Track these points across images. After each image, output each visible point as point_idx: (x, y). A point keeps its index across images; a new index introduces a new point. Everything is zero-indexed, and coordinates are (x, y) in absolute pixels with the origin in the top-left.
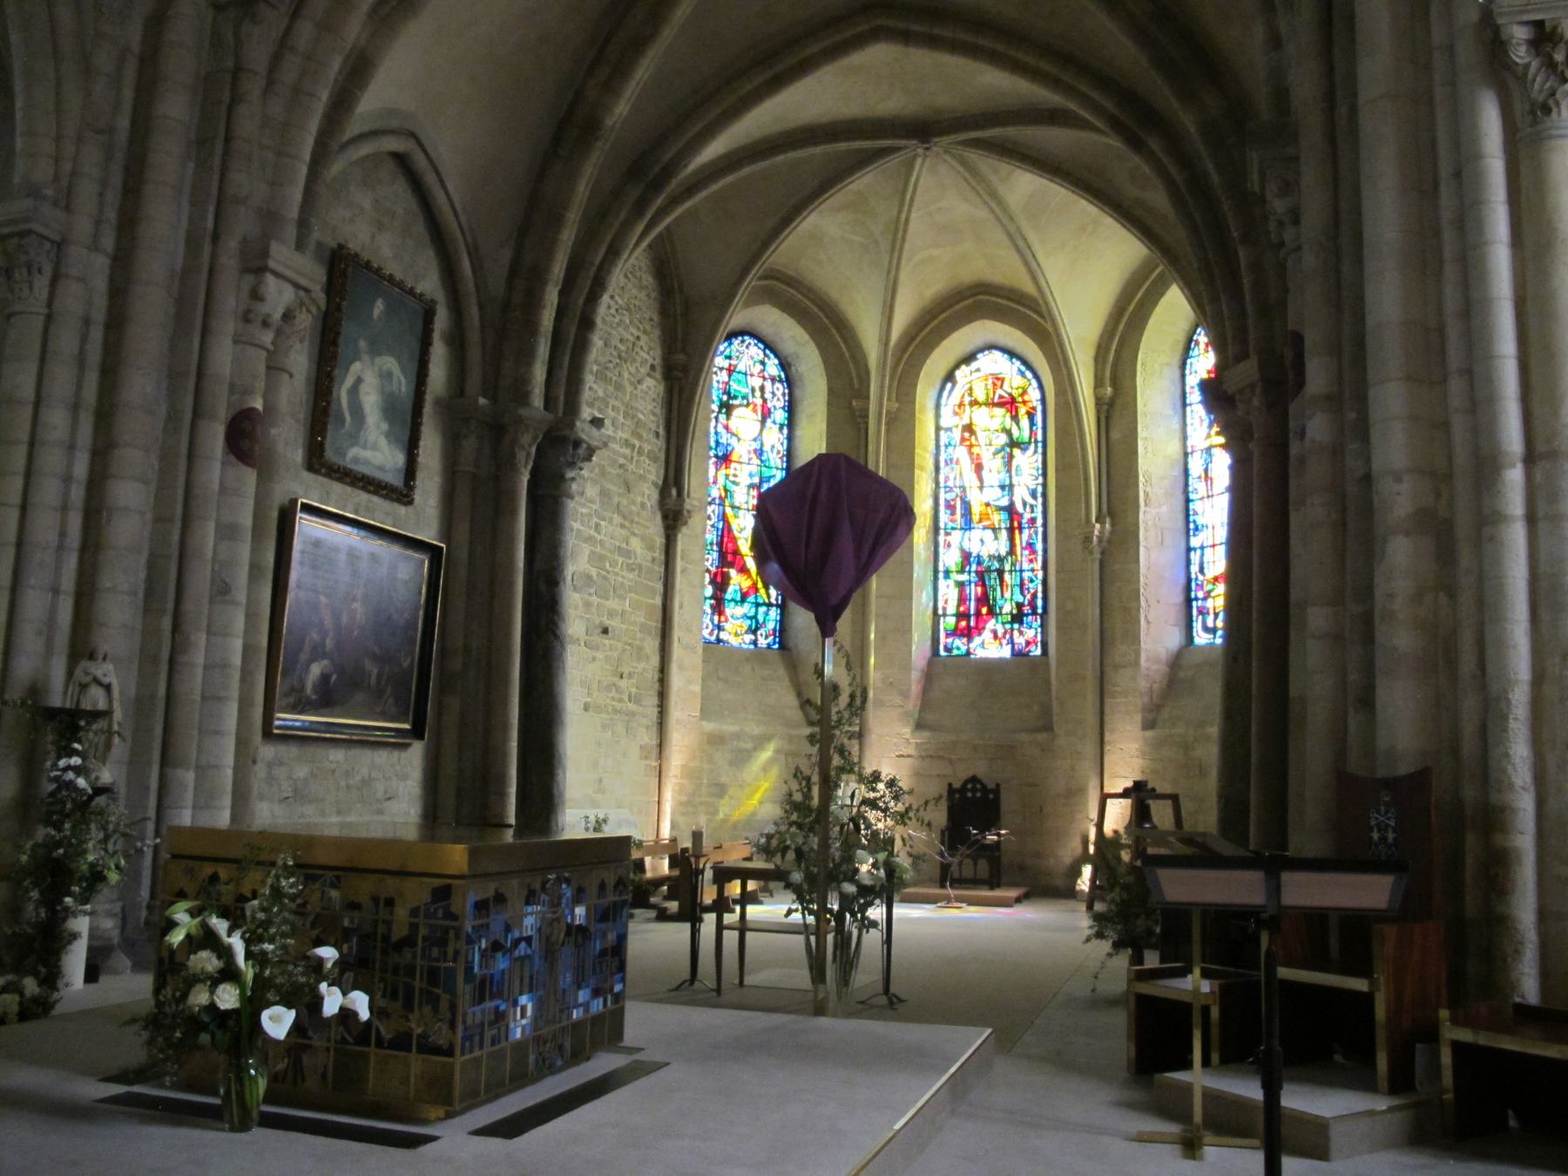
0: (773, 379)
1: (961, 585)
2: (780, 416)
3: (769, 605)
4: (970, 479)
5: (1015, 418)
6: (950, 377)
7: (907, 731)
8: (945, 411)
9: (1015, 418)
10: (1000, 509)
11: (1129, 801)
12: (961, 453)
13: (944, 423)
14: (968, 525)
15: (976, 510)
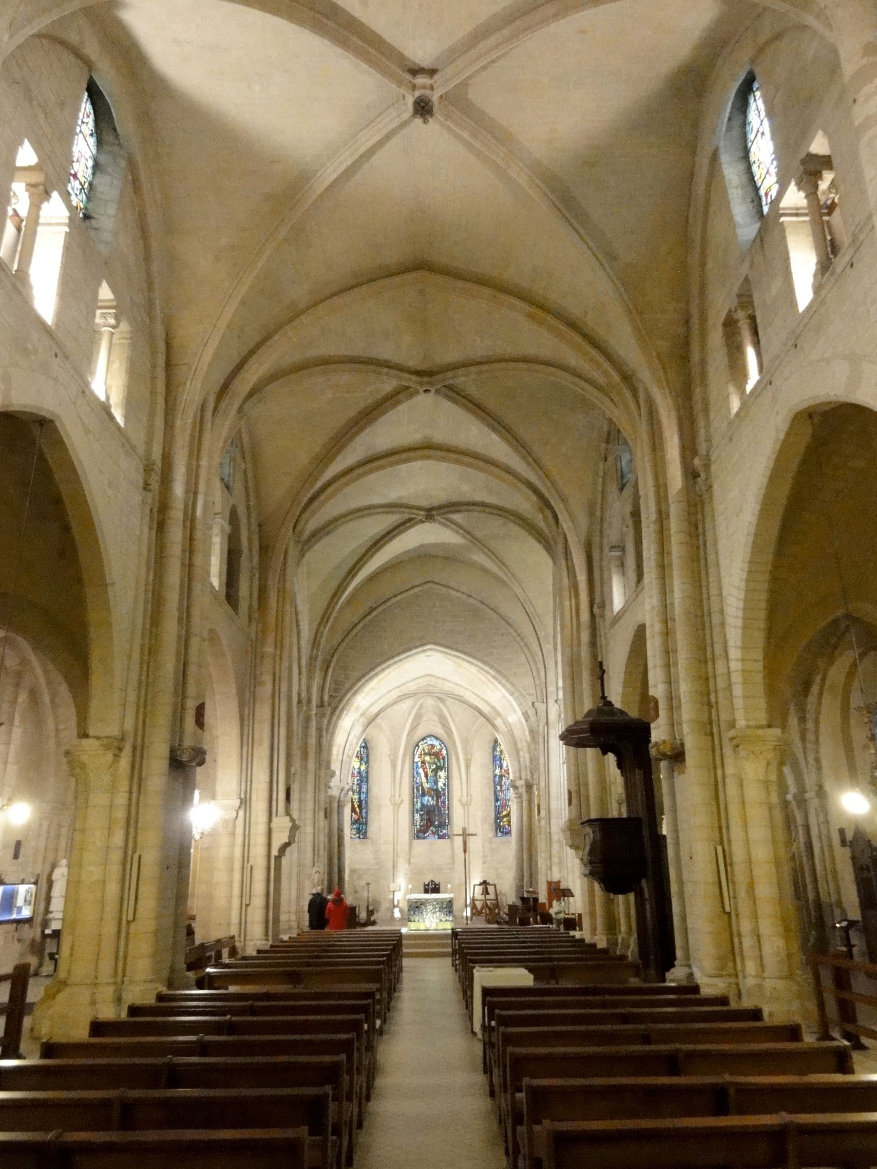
0: (364, 747)
1: (421, 815)
2: (365, 759)
3: (363, 824)
4: (424, 780)
5: (439, 760)
6: (417, 745)
7: (407, 866)
8: (416, 757)
9: (439, 760)
10: (434, 790)
11: (481, 887)
12: (421, 771)
13: (417, 759)
14: (423, 795)
15: (426, 790)
